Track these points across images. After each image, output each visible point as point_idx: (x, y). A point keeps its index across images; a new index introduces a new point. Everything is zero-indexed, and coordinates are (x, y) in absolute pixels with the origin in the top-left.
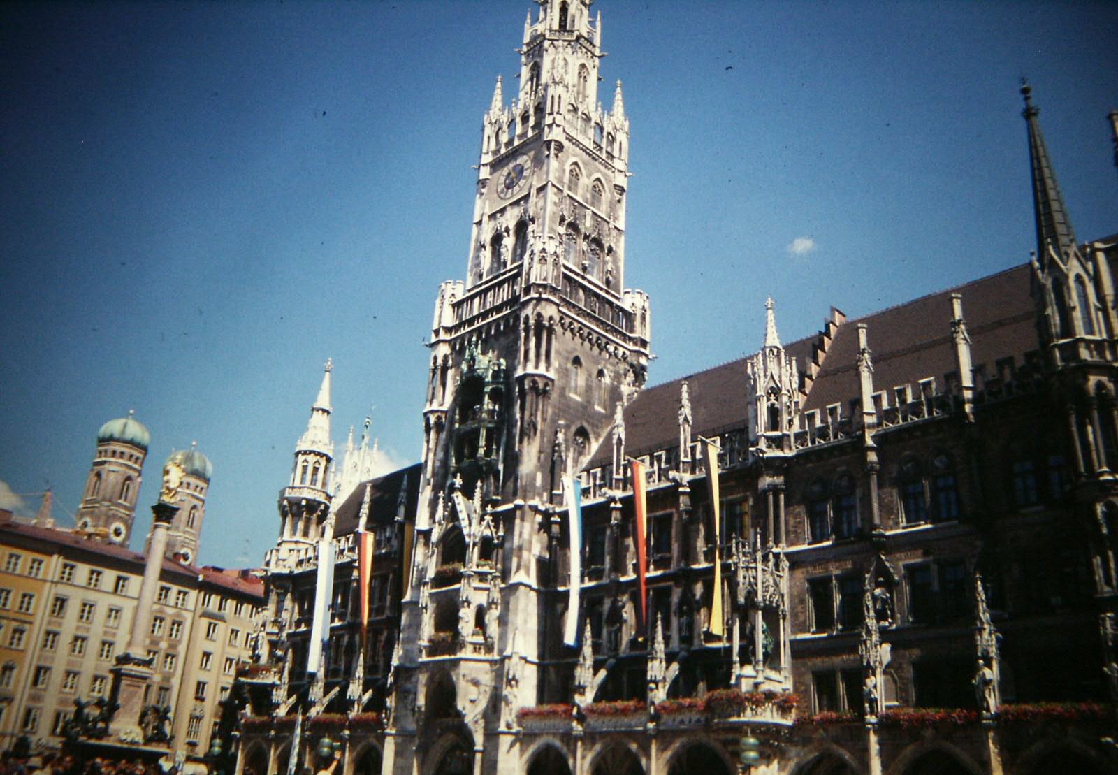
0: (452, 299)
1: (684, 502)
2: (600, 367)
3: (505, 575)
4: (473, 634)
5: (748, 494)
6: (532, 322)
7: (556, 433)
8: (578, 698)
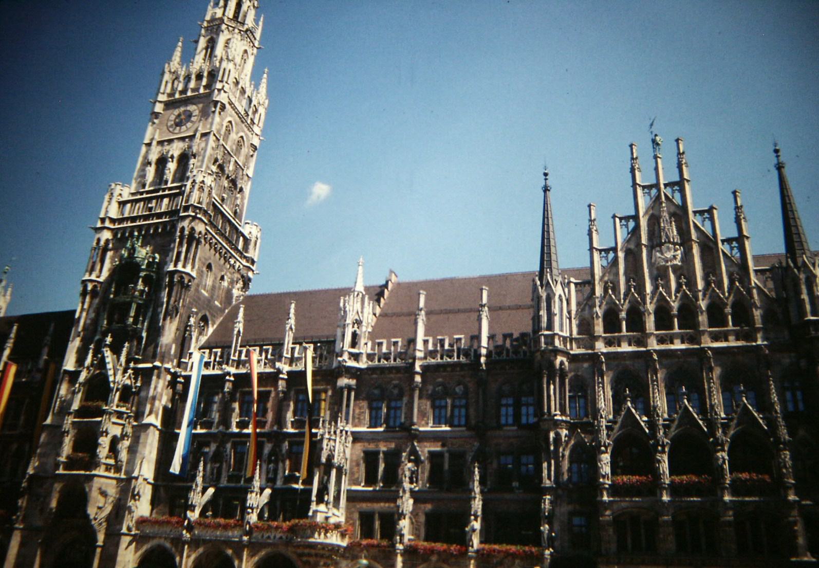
0: (119, 197)
1: (282, 385)
2: (223, 273)
3: (139, 415)
4: (107, 458)
5: (329, 387)
6: (186, 232)
7: (189, 317)
8: (189, 514)
